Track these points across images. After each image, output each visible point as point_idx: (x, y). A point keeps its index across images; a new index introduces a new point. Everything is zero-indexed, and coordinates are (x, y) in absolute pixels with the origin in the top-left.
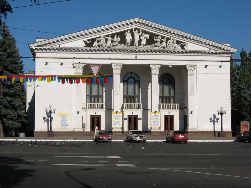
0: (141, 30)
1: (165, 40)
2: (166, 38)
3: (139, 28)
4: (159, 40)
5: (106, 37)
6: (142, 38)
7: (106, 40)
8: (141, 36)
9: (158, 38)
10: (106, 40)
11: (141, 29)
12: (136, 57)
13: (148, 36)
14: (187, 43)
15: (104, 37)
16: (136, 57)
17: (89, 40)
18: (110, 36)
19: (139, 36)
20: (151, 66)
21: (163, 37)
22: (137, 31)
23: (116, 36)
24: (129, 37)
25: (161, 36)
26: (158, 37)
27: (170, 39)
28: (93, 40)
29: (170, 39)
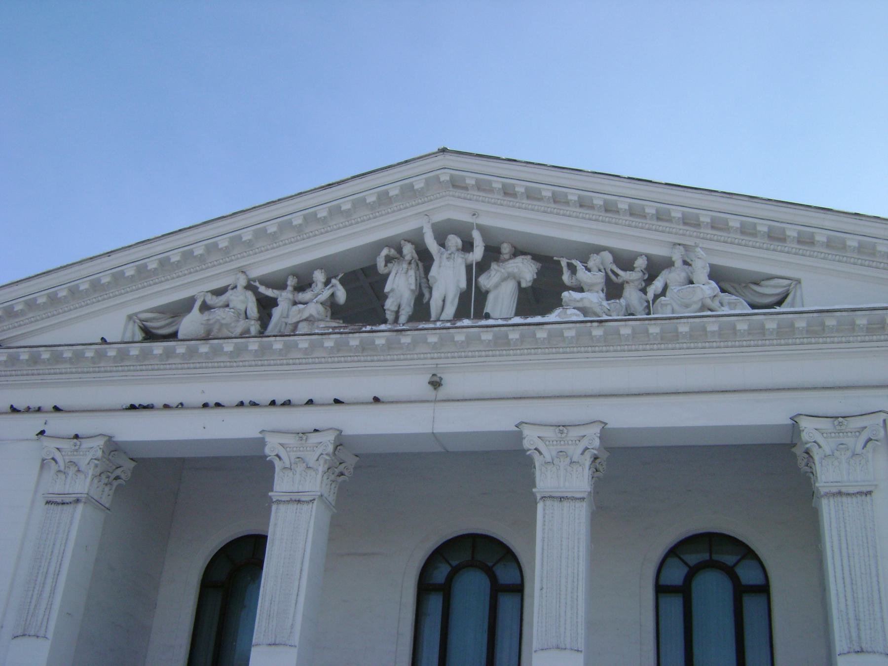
0: (476, 236)
1: (633, 277)
2: (641, 263)
3: (464, 217)
4: (597, 278)
5: (262, 289)
6: (486, 281)
7: (266, 305)
8: (483, 267)
9: (591, 264)
10: (266, 305)
11: (481, 228)
12: (436, 384)
13: (526, 270)
14: (798, 282)
15: (249, 287)
16: (436, 384)
17: (161, 310)
18: (291, 282)
19: (469, 268)
20: (531, 438)
21: (625, 262)
22: (454, 241)
23: (319, 277)
24: (400, 286)
25: (611, 251)
26: (584, 261)
27: (669, 264)
28: (185, 306)
29: (669, 264)
